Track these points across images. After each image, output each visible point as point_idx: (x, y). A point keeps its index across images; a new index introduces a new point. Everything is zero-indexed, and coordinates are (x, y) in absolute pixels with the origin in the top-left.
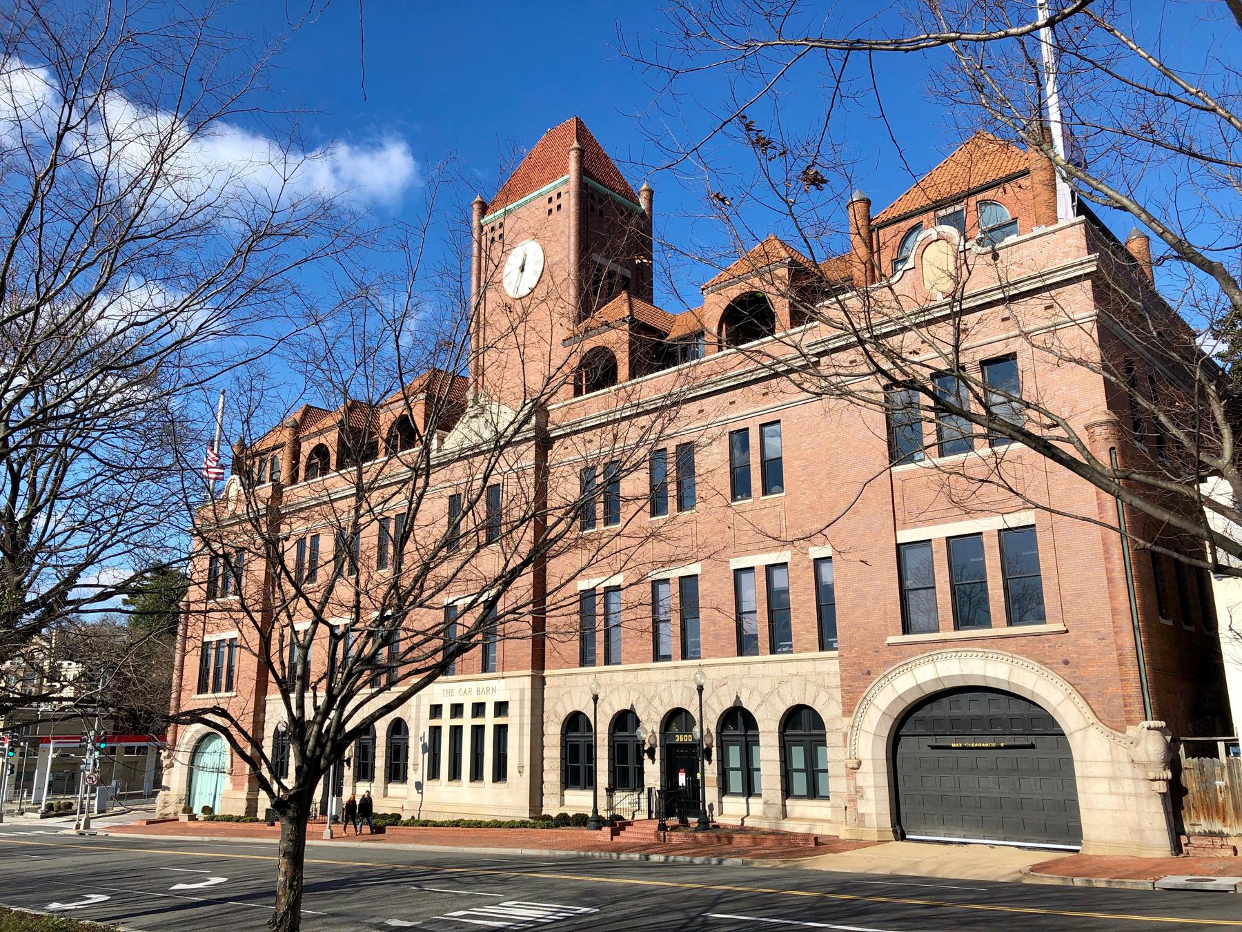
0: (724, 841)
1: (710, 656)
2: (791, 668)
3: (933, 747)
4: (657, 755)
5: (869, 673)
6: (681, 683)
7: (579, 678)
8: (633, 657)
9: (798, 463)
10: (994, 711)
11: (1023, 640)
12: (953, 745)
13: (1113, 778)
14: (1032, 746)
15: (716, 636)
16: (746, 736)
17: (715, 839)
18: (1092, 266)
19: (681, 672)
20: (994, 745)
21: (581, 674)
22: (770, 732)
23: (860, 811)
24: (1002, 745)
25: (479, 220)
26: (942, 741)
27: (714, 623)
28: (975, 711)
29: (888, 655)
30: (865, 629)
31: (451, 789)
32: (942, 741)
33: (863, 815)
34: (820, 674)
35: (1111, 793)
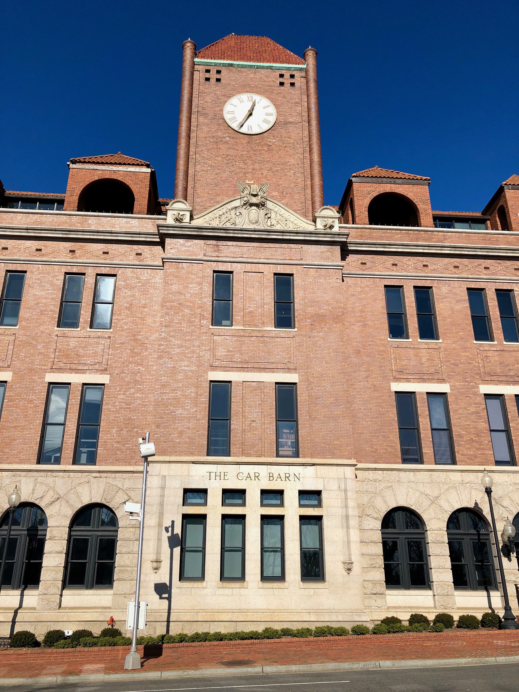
7: (402, 474)
8: (470, 459)
25: (193, 58)
31: (227, 591)
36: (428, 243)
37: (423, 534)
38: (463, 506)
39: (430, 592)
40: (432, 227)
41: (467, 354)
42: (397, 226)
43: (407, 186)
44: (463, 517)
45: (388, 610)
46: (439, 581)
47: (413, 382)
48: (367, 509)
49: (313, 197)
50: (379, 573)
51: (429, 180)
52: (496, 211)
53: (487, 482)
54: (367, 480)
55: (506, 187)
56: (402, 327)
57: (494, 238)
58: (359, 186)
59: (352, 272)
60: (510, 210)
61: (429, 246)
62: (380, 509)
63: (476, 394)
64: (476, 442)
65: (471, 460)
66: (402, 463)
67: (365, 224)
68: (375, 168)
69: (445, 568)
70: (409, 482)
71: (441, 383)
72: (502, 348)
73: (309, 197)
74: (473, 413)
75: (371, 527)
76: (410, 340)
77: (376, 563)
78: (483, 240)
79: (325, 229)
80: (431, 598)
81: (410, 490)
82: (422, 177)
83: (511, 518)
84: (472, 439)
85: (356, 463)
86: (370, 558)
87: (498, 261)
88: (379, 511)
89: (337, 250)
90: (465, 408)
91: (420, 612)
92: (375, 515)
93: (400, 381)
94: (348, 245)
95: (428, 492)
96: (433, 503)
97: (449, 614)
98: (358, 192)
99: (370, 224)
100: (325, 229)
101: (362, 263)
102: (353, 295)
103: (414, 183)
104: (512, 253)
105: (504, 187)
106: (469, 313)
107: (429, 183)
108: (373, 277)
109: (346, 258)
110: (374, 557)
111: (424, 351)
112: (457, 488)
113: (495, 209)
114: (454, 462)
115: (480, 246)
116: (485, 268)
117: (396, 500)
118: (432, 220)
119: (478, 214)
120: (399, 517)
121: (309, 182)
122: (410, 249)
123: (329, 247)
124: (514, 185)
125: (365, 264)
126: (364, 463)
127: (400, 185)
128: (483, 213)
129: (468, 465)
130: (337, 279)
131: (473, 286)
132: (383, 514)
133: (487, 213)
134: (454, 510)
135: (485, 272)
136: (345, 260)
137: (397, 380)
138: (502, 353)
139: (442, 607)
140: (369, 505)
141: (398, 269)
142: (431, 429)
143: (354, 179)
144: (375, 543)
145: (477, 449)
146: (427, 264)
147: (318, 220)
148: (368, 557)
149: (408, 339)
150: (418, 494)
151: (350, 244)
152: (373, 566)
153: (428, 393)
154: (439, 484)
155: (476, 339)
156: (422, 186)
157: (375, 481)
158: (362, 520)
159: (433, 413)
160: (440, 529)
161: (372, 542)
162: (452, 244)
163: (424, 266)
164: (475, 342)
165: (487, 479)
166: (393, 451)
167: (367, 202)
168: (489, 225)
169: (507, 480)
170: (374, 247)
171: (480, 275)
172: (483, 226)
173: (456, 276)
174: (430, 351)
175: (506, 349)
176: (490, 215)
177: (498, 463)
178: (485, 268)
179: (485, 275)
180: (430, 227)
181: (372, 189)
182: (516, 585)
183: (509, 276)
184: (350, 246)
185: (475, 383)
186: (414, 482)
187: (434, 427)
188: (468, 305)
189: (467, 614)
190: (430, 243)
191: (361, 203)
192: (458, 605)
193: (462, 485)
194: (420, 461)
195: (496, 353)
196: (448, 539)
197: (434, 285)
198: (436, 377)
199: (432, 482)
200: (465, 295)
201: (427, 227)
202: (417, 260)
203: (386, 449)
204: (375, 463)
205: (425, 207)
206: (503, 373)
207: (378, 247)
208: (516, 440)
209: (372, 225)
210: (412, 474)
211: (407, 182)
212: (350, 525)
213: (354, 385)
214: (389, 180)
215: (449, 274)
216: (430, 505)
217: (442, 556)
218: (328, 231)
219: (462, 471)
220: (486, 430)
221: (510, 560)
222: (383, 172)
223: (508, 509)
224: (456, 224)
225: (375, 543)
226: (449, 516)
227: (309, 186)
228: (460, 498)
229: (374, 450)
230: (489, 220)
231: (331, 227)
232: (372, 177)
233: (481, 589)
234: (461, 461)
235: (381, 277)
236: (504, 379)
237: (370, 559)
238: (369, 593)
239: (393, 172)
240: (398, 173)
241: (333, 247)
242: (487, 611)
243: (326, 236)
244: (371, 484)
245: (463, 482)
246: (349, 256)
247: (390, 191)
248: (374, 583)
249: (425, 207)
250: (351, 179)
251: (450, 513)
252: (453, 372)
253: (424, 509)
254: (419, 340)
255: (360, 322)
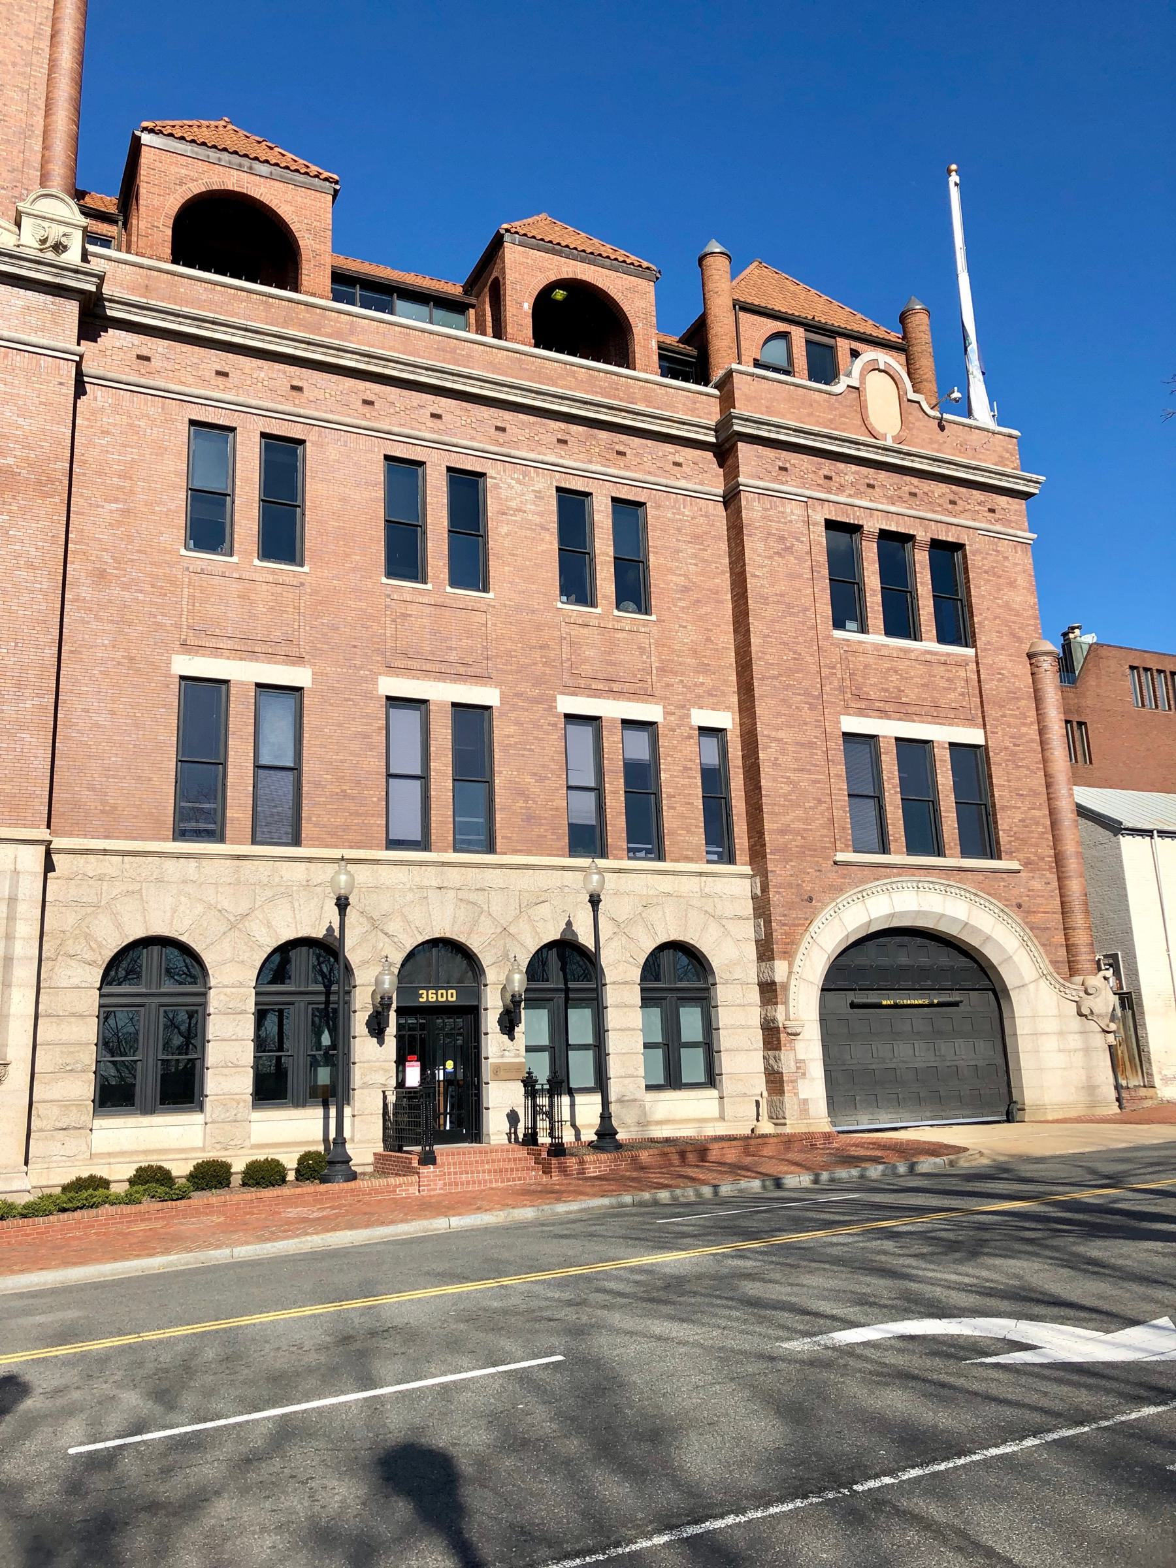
0: (691, 1157)
1: (516, 852)
2: (666, 884)
3: (853, 1006)
4: (391, 1030)
5: (810, 899)
6: (451, 894)
7: (169, 864)
9: (674, 578)
10: (924, 960)
11: (980, 877)
12: (884, 1003)
13: (1061, 1033)
14: (955, 1004)
15: (530, 819)
16: (567, 990)
17: (676, 1157)
18: (1037, 488)
19: (453, 875)
20: (927, 1002)
21: (178, 856)
22: (626, 983)
23: (802, 1096)
24: (936, 1001)
26: (872, 998)
27: (523, 793)
28: (903, 960)
29: (833, 876)
30: (803, 838)
32: (872, 998)
33: (806, 1101)
34: (708, 895)
35: (1060, 1051)
36: (307, 336)
37: (204, 994)
38: (300, 935)
39: (197, 1118)
40: (327, 298)
41: (363, 605)
42: (241, 279)
43: (282, 184)
44: (299, 957)
45: (91, 1162)
46: (221, 1093)
47: (228, 658)
48: (70, 942)
49: (45, 162)
50: (80, 1083)
51: (336, 182)
52: (487, 290)
53: (342, 884)
54: (79, 877)
55: (507, 237)
56: (222, 526)
57: (463, 350)
58: (157, 159)
59: (110, 375)
60: (508, 292)
61: (309, 343)
62: (104, 943)
63: (369, 695)
64: (353, 798)
65: (333, 837)
66: (174, 840)
67: (160, 259)
68: (222, 123)
69: (238, 1066)
70: (185, 882)
71: (293, 664)
72: (440, 601)
73: (36, 160)
74: (356, 735)
75: (75, 981)
76: (235, 559)
77: (77, 1062)
78: (438, 349)
79: (41, 250)
80: (200, 1129)
81: (183, 899)
82: (321, 171)
83: (398, 958)
84: (344, 791)
85: (48, 838)
86: (64, 1049)
87: (464, 404)
88: (100, 946)
89: (71, 309)
90: (340, 725)
91: (154, 1160)
92: (89, 956)
93: (197, 653)
94: (107, 304)
95: (225, 904)
96: (233, 927)
97: (224, 1160)
98: (152, 172)
99: (175, 261)
100: (41, 250)
101: (139, 357)
102: (107, 433)
103: (300, 182)
104: (495, 390)
105: (503, 236)
106: (380, 512)
107: (336, 191)
108: (164, 394)
109: (100, 336)
110: (72, 1050)
111: (265, 587)
112: (294, 895)
113: (485, 286)
114: (296, 842)
115: (425, 361)
116: (433, 415)
117: (145, 922)
118: (328, 281)
119: (454, 289)
120: (152, 957)
121: (39, 120)
122: (264, 341)
123: (50, 298)
124: (525, 235)
125: (148, 359)
126: (78, 836)
127: (262, 180)
128: (469, 287)
129: (327, 846)
130: (61, 384)
131: (400, 452)
132: (109, 954)
133: (472, 290)
134: (280, 943)
135: (431, 425)
136: (96, 341)
137: (188, 648)
138: (438, 611)
139: (218, 1146)
140: (77, 932)
141: (228, 385)
142: (258, 767)
143: (146, 138)
144: (81, 1016)
145: (351, 814)
146: (300, 384)
147: (25, 221)
148: (58, 1049)
149: (231, 555)
150: (200, 909)
151: (111, 301)
152: (68, 1068)
153: (258, 685)
154: (253, 887)
155: (390, 574)
156: (318, 194)
157: (101, 877)
158: (54, 966)
159: (265, 727)
160: (241, 985)
161: (73, 1015)
162: (363, 348)
163: (294, 388)
164: (384, 580)
165: (343, 878)
166: (154, 811)
167: (173, 203)
168: (472, 320)
169: (405, 880)
170: (174, 322)
171: (420, 430)
172: (458, 318)
173: (364, 423)
174: (279, 589)
175: (448, 602)
176: (478, 296)
177: (393, 844)
178: (433, 415)
179: (430, 432)
180: (321, 297)
181: (192, 174)
182: (384, 1092)
183: (480, 442)
184: (111, 308)
185: (371, 671)
186: (195, 882)
187: (264, 761)
188: (381, 494)
189: (265, 1157)
190: (311, 337)
191: (155, 203)
192: (254, 1139)
193: (305, 890)
194: (217, 836)
195: (428, 610)
196: (256, 1004)
197: (311, 437)
198: (283, 649)
199: (238, 882)
200: (378, 472)
201: (313, 295)
202: (279, 370)
203: (139, 807)
204: (107, 837)
205: (318, 246)
206: (433, 654)
207: (184, 324)
208: (438, 798)
209: (179, 264)
210: (193, 863)
211: (281, 176)
212: (14, 980)
213: (80, 653)
214: (236, 159)
215: (349, 416)
216: (224, 933)
217: (236, 1040)
218: (50, 256)
219: (310, 860)
220: (378, 773)
221: (381, 1042)
222: (231, 136)
223: (396, 940)
224: (400, 305)
225: (81, 1016)
226: (265, 956)
227: (39, 131)
228: (298, 917)
229: (107, 808)
230: (473, 306)
231: (59, 248)
232: (193, 141)
233: (314, 1105)
234: (312, 839)
235: (185, 399)
236: (436, 667)
237: (62, 1052)
238: (48, 1127)
239: (259, 142)
240: (271, 148)
241: (58, 299)
242: (313, 1149)
243: (41, 267)
244: (89, 886)
245: (310, 883)
246: (107, 332)
247: (236, 189)
248: (77, 1104)
249: (318, 246)
250: (138, 133)
251: (269, 950)
252: (328, 643)
253: (209, 941)
254: (257, 562)
255: (116, 500)
